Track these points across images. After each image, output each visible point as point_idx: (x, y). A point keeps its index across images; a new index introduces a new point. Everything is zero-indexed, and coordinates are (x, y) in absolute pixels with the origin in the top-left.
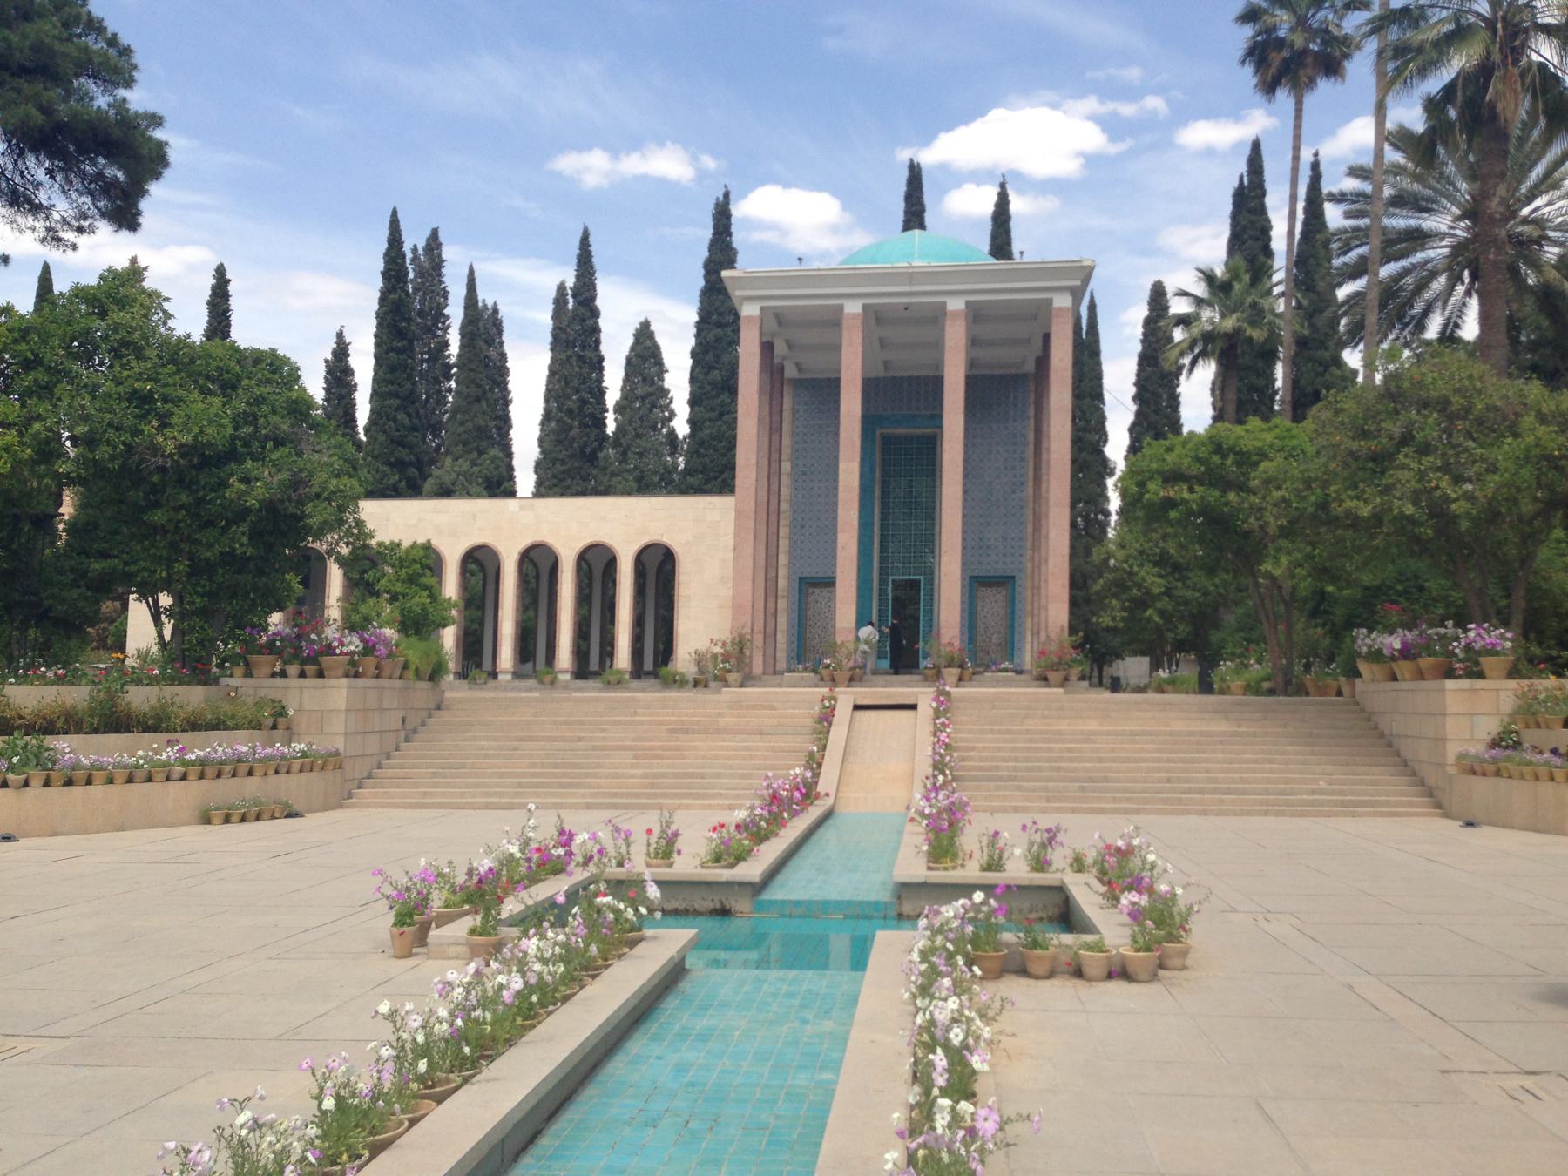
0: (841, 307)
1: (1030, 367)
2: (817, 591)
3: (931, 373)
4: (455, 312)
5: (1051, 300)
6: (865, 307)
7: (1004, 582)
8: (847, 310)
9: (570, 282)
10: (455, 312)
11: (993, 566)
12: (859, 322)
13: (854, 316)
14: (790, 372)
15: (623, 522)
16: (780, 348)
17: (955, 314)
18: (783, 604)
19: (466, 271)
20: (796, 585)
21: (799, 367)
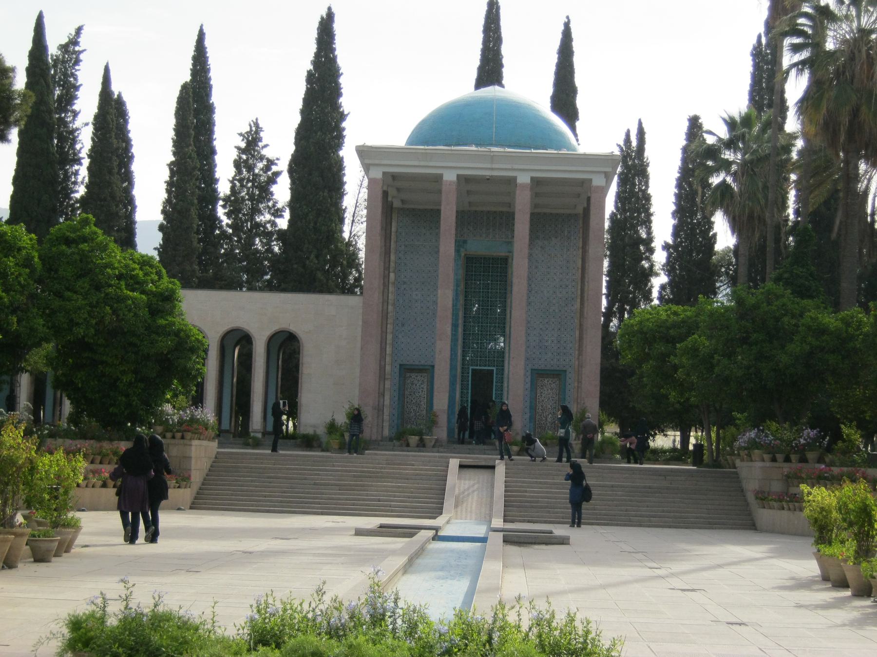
0: (441, 176)
1: (580, 210)
2: (413, 375)
3: (505, 209)
4: (86, 106)
5: (591, 180)
6: (458, 176)
7: (558, 375)
8: (445, 178)
9: (188, 78)
10: (86, 106)
12: (454, 187)
13: (451, 183)
14: (397, 204)
15: (259, 312)
16: (392, 192)
17: (523, 186)
18: (388, 384)
19: (102, 72)
20: (397, 370)
21: (403, 201)
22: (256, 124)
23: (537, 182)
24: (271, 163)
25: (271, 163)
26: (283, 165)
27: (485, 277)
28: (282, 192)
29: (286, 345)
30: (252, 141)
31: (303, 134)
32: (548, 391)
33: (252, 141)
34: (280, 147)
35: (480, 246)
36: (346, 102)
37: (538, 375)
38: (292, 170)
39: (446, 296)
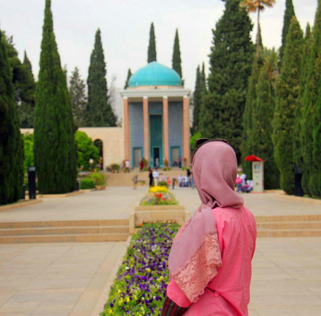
11: (175, 144)
22: (76, 68)
23: (169, 98)
24: (82, 82)
25: (82, 82)
26: (85, 83)
27: (156, 120)
28: (86, 91)
29: (99, 143)
30: (76, 75)
31: (91, 69)
32: (176, 152)
33: (76, 75)
34: (84, 76)
35: (154, 113)
36: (106, 60)
37: (172, 148)
38: (88, 82)
39: (146, 130)
